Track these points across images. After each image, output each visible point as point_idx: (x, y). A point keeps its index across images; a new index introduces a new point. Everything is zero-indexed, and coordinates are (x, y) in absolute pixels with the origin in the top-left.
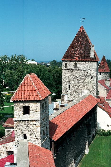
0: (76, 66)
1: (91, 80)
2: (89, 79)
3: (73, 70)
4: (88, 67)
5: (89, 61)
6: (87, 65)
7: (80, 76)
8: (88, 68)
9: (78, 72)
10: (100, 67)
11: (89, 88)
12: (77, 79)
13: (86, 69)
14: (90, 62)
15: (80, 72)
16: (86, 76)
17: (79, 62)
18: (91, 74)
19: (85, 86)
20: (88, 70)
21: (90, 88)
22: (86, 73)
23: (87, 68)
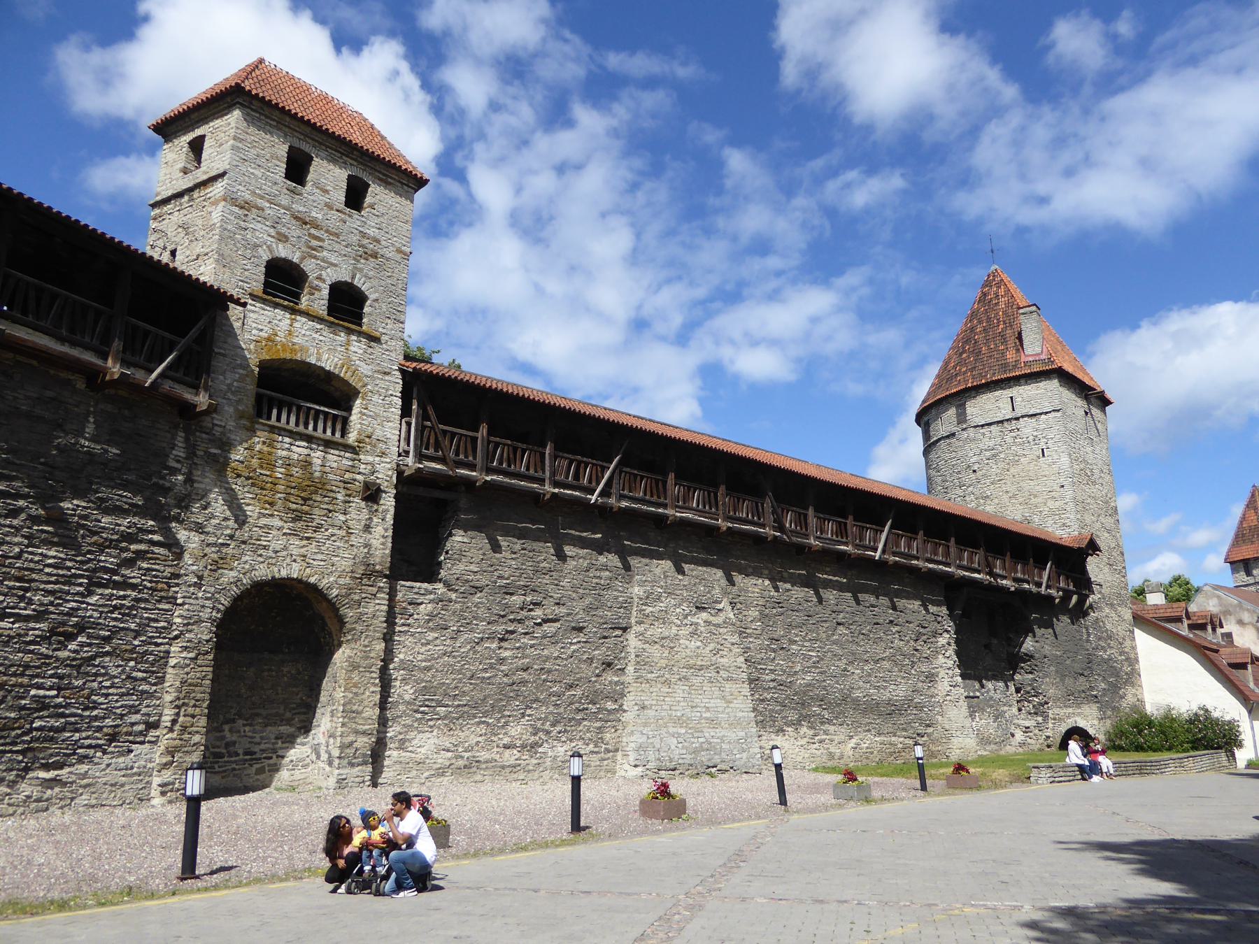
0: (962, 418)
3: (953, 435)
8: (1018, 413)
11: (1034, 500)
12: (974, 471)
14: (1022, 381)
18: (1035, 434)
19: (1014, 496)
20: (1017, 419)
21: (1040, 500)
22: (1014, 434)
23: (1014, 410)
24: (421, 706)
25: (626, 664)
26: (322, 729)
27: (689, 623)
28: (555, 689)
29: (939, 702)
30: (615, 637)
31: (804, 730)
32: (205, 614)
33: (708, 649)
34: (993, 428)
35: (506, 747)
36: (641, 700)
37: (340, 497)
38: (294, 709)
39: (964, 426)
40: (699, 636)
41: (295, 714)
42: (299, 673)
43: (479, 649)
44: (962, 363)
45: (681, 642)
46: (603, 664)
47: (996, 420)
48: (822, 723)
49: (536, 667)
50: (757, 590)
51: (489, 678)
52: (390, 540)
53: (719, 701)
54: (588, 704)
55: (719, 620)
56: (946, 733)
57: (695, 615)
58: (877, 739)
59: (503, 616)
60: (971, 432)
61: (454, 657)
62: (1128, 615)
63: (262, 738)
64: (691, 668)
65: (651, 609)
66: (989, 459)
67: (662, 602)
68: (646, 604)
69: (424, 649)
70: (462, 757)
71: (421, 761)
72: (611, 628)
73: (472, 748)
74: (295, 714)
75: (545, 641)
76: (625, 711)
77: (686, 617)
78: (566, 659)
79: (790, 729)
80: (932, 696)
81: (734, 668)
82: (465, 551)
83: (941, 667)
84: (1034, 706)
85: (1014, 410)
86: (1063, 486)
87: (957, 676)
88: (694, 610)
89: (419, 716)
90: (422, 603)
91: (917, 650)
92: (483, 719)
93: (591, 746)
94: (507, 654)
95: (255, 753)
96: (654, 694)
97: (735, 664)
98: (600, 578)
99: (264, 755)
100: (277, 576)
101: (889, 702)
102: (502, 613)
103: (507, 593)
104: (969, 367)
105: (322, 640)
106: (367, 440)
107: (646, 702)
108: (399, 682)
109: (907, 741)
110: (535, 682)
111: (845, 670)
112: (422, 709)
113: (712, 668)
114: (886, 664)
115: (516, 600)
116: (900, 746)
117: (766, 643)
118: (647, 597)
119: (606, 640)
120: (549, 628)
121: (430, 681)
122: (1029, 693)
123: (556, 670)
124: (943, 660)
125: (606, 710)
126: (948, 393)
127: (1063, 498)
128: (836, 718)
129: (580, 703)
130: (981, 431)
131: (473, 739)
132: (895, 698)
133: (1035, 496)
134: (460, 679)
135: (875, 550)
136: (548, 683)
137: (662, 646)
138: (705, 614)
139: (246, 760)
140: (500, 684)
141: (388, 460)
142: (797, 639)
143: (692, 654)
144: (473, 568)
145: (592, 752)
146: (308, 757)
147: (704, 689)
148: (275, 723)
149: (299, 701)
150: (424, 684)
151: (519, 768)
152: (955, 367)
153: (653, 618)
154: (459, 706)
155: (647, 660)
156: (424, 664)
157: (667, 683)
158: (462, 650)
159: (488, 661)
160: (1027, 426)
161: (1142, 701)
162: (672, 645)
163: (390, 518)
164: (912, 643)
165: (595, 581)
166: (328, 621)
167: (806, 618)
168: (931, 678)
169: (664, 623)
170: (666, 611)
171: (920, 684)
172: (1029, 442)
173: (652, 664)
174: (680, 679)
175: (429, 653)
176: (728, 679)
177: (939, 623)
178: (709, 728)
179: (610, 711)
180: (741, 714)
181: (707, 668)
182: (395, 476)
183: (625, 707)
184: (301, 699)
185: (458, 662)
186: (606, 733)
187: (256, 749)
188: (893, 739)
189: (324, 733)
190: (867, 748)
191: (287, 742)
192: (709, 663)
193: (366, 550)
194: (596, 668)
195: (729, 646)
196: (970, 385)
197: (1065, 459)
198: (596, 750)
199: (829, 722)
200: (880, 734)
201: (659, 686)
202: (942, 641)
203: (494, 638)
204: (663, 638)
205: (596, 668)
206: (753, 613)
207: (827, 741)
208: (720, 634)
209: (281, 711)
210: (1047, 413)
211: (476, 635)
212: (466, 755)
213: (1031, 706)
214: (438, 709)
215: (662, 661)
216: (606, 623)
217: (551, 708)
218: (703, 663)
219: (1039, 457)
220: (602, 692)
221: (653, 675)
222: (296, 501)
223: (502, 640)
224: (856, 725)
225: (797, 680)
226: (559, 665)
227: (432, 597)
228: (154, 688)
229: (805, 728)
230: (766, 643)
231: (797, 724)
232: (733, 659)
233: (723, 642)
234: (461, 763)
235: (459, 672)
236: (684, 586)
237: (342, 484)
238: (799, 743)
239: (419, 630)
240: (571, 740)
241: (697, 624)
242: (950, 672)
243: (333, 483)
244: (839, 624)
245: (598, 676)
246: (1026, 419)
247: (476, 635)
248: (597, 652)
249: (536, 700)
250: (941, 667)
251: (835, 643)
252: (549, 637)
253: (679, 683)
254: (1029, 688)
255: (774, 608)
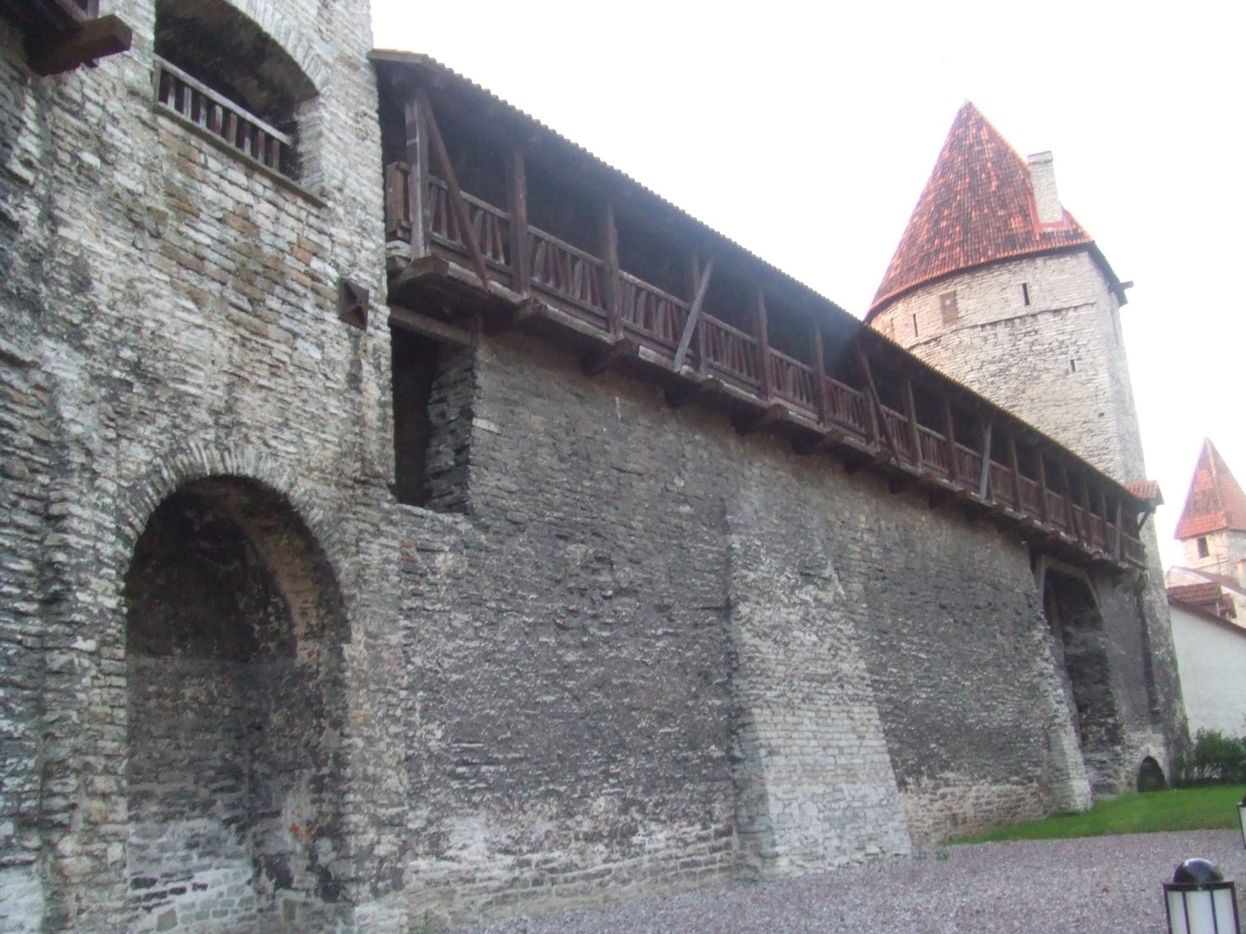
0: (950, 313)
1: (1070, 376)
2: (1056, 372)
3: (936, 339)
4: (1033, 301)
5: (1032, 256)
6: (1024, 286)
7: (986, 367)
8: (1036, 306)
9: (971, 346)
10: (1196, 503)
13: (1029, 310)
14: (1039, 262)
15: (985, 339)
16: (1030, 359)
17: (967, 278)
18: (1061, 338)
20: (1034, 316)
22: (1028, 339)
23: (1027, 302)
24: (457, 764)
25: (730, 676)
26: (288, 817)
27: (798, 601)
28: (643, 724)
29: (1043, 728)
30: (710, 624)
31: (925, 781)
32: (108, 551)
33: (827, 646)
34: (1002, 331)
35: (591, 838)
36: (767, 739)
37: (308, 306)
38: (213, 780)
39: (954, 327)
40: (813, 625)
41: (215, 791)
42: (213, 702)
43: (533, 647)
44: (938, 233)
45: (796, 633)
46: (700, 674)
47: (1004, 317)
48: (942, 768)
49: (615, 681)
50: (858, 549)
51: (553, 704)
52: (390, 412)
53: (851, 736)
54: (687, 749)
55: (828, 597)
56: (1058, 774)
57: (801, 587)
58: (994, 788)
59: (558, 582)
60: (965, 336)
61: (499, 663)
62: (1166, 603)
63: (163, 848)
64: (812, 680)
65: (752, 576)
66: (994, 375)
67: (762, 563)
68: (745, 566)
69: (450, 646)
70: (528, 863)
71: (468, 876)
72: (704, 609)
73: (541, 844)
74: (215, 791)
75: (622, 633)
76: (735, 760)
77: (793, 589)
78: (653, 667)
79: (910, 780)
80: (1036, 720)
81: (857, 680)
82: (494, 450)
83: (1041, 674)
84: (1107, 730)
85: (1027, 302)
86: (1102, 415)
87: (1058, 687)
88: (800, 579)
89: (455, 784)
90: (440, 551)
91: (1016, 649)
92: (551, 787)
93: (698, 827)
94: (571, 657)
95: (153, 882)
96: (779, 727)
97: (857, 672)
98: (679, 515)
99: (171, 886)
100: (220, 469)
101: (1000, 731)
102: (559, 577)
103: (560, 537)
104: (957, 240)
105: (257, 628)
106: (338, 195)
107: (772, 742)
108: (417, 715)
109: (1020, 789)
110: (615, 710)
111: (956, 682)
112: (461, 770)
113: (834, 679)
114: (991, 672)
115: (576, 551)
116: (1014, 797)
117: (876, 637)
118: (745, 553)
119: (699, 631)
120: (625, 607)
121: (466, 712)
122: (1099, 710)
123: (642, 687)
124: (1044, 664)
125: (710, 759)
126: (927, 277)
127: (1102, 432)
128: (954, 758)
129: (677, 747)
130: (982, 334)
131: (542, 826)
132: (1005, 724)
133: (1065, 429)
134: (511, 706)
135: (977, 489)
136: (634, 713)
137: (775, 642)
138: (811, 587)
139: (138, 899)
140: (569, 715)
141: (373, 246)
142: (905, 631)
143: (808, 655)
144: (507, 483)
145: (701, 839)
146: (249, 882)
147: (834, 715)
148: (182, 813)
149: (219, 763)
150: (458, 719)
151: (607, 877)
152: (930, 240)
153: (757, 592)
154: (514, 760)
155: (763, 666)
156: (455, 677)
157: (790, 705)
158: (509, 649)
159: (547, 671)
160: (1049, 329)
161: (1185, 718)
162: (786, 639)
163: (386, 363)
164: (1012, 639)
165: (675, 521)
166: (286, 586)
167: (910, 596)
168: (1033, 691)
169: (770, 601)
170: (770, 579)
171: (1024, 702)
172: (1051, 350)
173: (770, 673)
174: (803, 700)
175: (461, 655)
176: (855, 699)
177: (1030, 606)
178: (847, 782)
179: (717, 762)
180: (877, 758)
181: (830, 680)
182: (384, 279)
183: (737, 753)
184: (224, 759)
185: (506, 673)
186: (714, 801)
187: (154, 872)
188: (1008, 786)
189: (294, 829)
190: (988, 803)
191: (209, 853)
192: (830, 671)
193: (357, 429)
194: (692, 682)
195: (845, 641)
196: (962, 265)
197: (1103, 377)
198: (704, 833)
199: (945, 766)
200: (996, 781)
201: (782, 711)
202: (1038, 635)
203: (549, 625)
204: (774, 627)
205: (692, 682)
206: (857, 586)
207: (949, 797)
208: (834, 621)
209: (191, 787)
210: (1076, 308)
211: (526, 619)
212: (536, 857)
213: (1103, 731)
214: (484, 769)
215: (781, 668)
216: (695, 599)
217: (643, 761)
218: (824, 672)
219: (1067, 373)
220: (703, 727)
221: (774, 693)
222: (240, 303)
223: (562, 628)
224: (978, 772)
225: (912, 698)
226: (643, 678)
227: (452, 538)
228: (21, 726)
229: (925, 778)
230: (876, 637)
231: (915, 772)
232: (852, 665)
233: (839, 634)
234: (529, 874)
235: (507, 692)
236: (784, 537)
237: (308, 281)
238: (923, 802)
239: (439, 606)
240: (672, 818)
241: (804, 603)
242: (1051, 681)
243: (295, 274)
244: (942, 607)
245: (695, 697)
246: (1047, 316)
247: (526, 619)
248: (689, 654)
249: (622, 745)
250: (1041, 674)
251: (943, 638)
252: (625, 624)
253: (803, 706)
254: (1099, 705)
255: (877, 579)
